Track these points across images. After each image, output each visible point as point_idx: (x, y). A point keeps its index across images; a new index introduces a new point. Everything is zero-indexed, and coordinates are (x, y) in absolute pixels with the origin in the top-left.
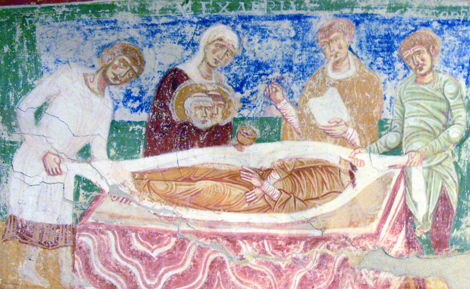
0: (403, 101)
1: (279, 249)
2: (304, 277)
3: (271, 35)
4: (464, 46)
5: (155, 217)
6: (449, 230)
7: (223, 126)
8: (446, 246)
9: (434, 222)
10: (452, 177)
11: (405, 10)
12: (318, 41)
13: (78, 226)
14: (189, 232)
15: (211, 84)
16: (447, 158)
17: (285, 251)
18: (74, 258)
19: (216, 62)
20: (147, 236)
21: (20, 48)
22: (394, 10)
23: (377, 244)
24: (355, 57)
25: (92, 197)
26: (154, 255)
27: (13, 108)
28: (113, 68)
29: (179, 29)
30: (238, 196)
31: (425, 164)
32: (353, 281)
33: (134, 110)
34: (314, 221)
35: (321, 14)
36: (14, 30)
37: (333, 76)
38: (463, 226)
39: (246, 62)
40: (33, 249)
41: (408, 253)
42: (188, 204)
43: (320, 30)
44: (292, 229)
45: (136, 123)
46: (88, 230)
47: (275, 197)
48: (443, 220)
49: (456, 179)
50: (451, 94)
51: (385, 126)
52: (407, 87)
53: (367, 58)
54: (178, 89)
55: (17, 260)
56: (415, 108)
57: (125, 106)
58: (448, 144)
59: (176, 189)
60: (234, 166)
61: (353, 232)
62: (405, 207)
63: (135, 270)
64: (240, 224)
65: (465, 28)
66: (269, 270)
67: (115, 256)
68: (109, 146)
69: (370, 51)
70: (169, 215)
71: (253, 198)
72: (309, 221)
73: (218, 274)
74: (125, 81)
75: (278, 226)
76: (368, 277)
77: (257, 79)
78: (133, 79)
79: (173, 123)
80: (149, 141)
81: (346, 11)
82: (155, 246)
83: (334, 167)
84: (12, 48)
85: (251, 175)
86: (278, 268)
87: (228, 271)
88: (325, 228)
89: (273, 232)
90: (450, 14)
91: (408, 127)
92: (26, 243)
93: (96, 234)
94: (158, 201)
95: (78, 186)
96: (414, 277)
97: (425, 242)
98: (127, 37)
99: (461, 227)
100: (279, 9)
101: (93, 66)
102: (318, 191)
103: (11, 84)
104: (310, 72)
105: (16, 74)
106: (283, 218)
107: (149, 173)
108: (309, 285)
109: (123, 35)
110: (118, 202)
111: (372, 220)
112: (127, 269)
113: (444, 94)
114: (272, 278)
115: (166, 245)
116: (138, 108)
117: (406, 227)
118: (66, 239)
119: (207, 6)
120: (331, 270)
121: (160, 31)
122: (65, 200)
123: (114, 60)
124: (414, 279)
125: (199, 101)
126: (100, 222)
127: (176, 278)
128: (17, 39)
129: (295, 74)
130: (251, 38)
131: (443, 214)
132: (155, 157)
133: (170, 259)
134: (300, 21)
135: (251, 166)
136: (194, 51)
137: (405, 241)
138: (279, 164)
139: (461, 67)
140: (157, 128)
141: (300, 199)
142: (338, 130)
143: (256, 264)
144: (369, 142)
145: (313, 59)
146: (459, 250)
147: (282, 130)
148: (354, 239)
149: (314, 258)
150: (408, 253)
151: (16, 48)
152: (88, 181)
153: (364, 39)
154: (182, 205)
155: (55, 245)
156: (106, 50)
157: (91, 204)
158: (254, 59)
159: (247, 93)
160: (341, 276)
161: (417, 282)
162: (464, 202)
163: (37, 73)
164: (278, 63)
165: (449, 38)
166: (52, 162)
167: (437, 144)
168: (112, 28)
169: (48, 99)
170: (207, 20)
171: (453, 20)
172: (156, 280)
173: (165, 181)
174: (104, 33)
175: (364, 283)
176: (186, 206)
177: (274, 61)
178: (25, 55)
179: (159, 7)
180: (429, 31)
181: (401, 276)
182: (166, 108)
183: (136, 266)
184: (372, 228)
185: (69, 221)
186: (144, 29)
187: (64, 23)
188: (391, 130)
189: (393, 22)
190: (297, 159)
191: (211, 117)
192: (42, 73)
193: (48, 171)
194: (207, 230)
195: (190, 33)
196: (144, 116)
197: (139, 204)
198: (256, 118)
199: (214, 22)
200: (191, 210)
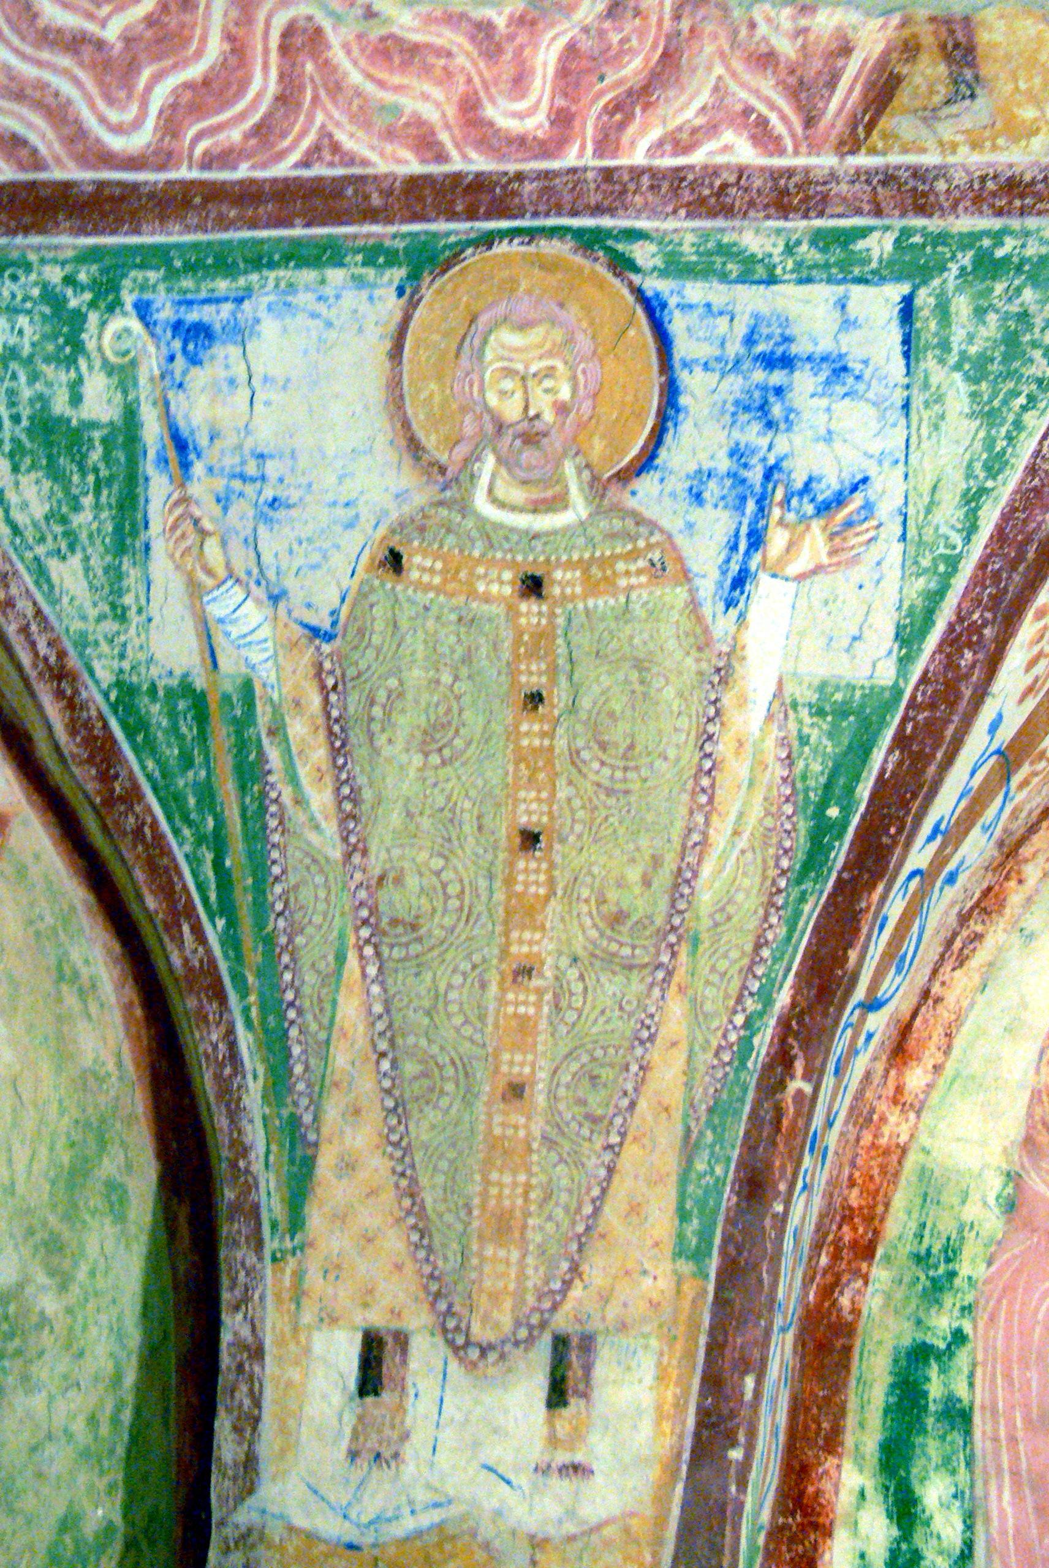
2: (571, 49)
26: (112, 33)
32: (726, 48)
63: (67, 88)
66: (461, 39)
73: (309, 67)
82: (106, 9)
86: (483, 31)
87: (337, 54)
96: (934, 13)
108: (589, 70)
112: (42, 86)
114: (474, 63)
120: (654, 19)
124: (933, 19)
133: (159, 41)
172: (134, 109)
175: (764, 49)
181: (887, 13)
183: (66, 73)
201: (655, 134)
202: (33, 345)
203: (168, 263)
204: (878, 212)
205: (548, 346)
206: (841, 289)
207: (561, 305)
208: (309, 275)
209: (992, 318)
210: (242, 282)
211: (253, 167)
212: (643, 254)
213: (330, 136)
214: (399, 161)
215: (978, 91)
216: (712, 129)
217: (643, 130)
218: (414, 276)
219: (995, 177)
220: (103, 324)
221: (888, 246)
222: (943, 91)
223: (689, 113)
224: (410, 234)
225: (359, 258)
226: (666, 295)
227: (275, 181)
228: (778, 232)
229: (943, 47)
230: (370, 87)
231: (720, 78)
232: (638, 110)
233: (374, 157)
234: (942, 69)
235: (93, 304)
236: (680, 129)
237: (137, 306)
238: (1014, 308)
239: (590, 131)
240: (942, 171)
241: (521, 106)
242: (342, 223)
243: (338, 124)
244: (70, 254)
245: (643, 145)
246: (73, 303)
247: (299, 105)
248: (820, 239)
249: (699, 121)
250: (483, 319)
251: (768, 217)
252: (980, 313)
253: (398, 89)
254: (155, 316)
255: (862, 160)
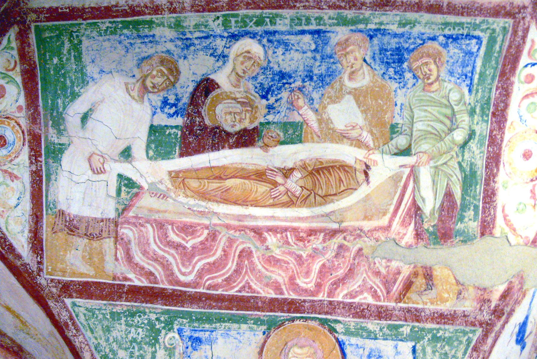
0: (412, 107)
1: (301, 240)
2: (324, 265)
3: (293, 48)
4: (467, 58)
5: (189, 211)
6: (454, 223)
7: (251, 130)
8: (450, 238)
9: (441, 216)
10: (456, 176)
11: (414, 25)
12: (336, 53)
13: (120, 220)
14: (220, 225)
15: (239, 92)
16: (451, 158)
17: (306, 242)
18: (116, 249)
19: (244, 72)
20: (182, 228)
21: (68, 59)
22: (404, 25)
23: (389, 235)
24: (369, 68)
25: (133, 193)
26: (189, 245)
27: (61, 113)
28: (152, 78)
29: (211, 43)
30: (264, 192)
31: (432, 163)
33: (171, 116)
34: (332, 215)
35: (338, 29)
36: (63, 43)
37: (350, 85)
38: (466, 219)
39: (271, 73)
40: (79, 240)
41: (417, 244)
42: (219, 199)
43: (337, 44)
44: (312, 222)
45: (172, 127)
46: (129, 223)
47: (297, 193)
48: (448, 214)
49: (460, 179)
50: (455, 101)
51: (396, 130)
52: (416, 95)
53: (380, 69)
54: (210, 96)
55: (66, 250)
56: (423, 114)
57: (163, 112)
58: (452, 146)
59: (208, 186)
60: (260, 165)
61: (367, 225)
62: (414, 202)
63: (171, 259)
64: (266, 218)
65: (468, 42)
66: (292, 259)
67: (154, 246)
68: (148, 147)
69: (383, 62)
70: (202, 209)
71: (278, 194)
72: (328, 215)
73: (246, 262)
74: (163, 90)
75: (300, 219)
76: (381, 265)
77: (281, 87)
78: (170, 88)
79: (206, 127)
80: (184, 143)
81: (361, 26)
82: (189, 238)
83: (350, 167)
84: (60, 59)
85: (275, 173)
87: (255, 260)
88: (342, 222)
89: (295, 224)
90: (454, 29)
91: (416, 131)
92: (74, 235)
93: (136, 227)
94: (192, 197)
95: (120, 183)
97: (432, 234)
98: (164, 49)
99: (464, 221)
100: (301, 25)
101: (134, 76)
102: (336, 188)
103: (60, 92)
104: (328, 81)
105: (64, 83)
106: (304, 212)
107: (184, 172)
108: (327, 272)
109: (160, 48)
110: (156, 198)
111: (384, 214)
112: (164, 258)
113: (449, 101)
114: (295, 266)
115: (199, 236)
116: (174, 114)
117: (415, 220)
118: (109, 232)
119: (236, 22)
120: (348, 259)
121: (193, 45)
122: (108, 196)
123: (153, 70)
124: (422, 267)
125: (229, 107)
126: (140, 216)
127: (208, 266)
128: (65, 52)
129: (315, 83)
130: (276, 50)
131: (449, 209)
132: (190, 157)
133: (203, 249)
134: (319, 36)
135: (276, 165)
136: (224, 63)
137: (414, 232)
138: (301, 164)
139: (464, 77)
140: (191, 132)
141: (320, 196)
142: (354, 134)
143: (280, 253)
144: (381, 145)
145: (331, 70)
146: (462, 241)
147: (303, 133)
148: (368, 231)
149: (332, 248)
150: (417, 244)
151: (64, 59)
152: (129, 180)
153: (377, 52)
154: (214, 201)
155: (99, 237)
156: (145, 61)
157: (132, 200)
158: (278, 70)
159: (272, 100)
160: (356, 264)
161: (424, 270)
162: (467, 198)
163: (83, 82)
164: (300, 73)
165: (454, 51)
166: (97, 162)
167: (442, 146)
168: (151, 42)
169: (93, 105)
170: (236, 35)
171: (457, 34)
173: (198, 179)
174: (143, 46)
175: (377, 271)
176: (217, 201)
177: (296, 71)
178: (72, 66)
179: (193, 23)
180: (435, 44)
182: (199, 113)
184: (384, 221)
185: (112, 215)
186: (179, 43)
187: (108, 37)
188: (401, 134)
189: (403, 36)
190: (317, 159)
191: (240, 121)
192: (88, 82)
193: (93, 170)
194: (236, 223)
195: (221, 47)
196: (179, 121)
197: (174, 200)
198: (280, 123)
199: (243, 36)
200: (221, 205)
201: (345, 292)
202: (142, 338)
203: (191, 318)
204: (406, 320)
205: (309, 353)
206: (396, 342)
207: (314, 341)
208: (235, 326)
209: (437, 354)
210: (214, 325)
211: (223, 291)
212: (339, 327)
213: (249, 283)
214: (268, 293)
215: (433, 288)
216: (362, 292)
217: (341, 291)
218: (269, 329)
219: (437, 313)
220: (167, 334)
221: (409, 330)
222: (424, 287)
223: (355, 287)
224: (269, 316)
225: (252, 322)
226: (345, 341)
227: (229, 295)
228: (378, 324)
229: (424, 275)
230: (263, 270)
231: (365, 277)
232: (341, 285)
233: (261, 291)
234: (424, 281)
235: (164, 328)
236: (352, 291)
237: (178, 330)
238: (443, 352)
239: (326, 290)
240: (423, 310)
241: (307, 280)
242: (248, 311)
243: (252, 280)
244: (160, 311)
245: (341, 295)
246: (158, 327)
247: (241, 273)
248: (390, 327)
249: (358, 290)
250: (289, 344)
251: (375, 319)
252: (434, 352)
253: (271, 271)
254: (184, 334)
255: (402, 305)
